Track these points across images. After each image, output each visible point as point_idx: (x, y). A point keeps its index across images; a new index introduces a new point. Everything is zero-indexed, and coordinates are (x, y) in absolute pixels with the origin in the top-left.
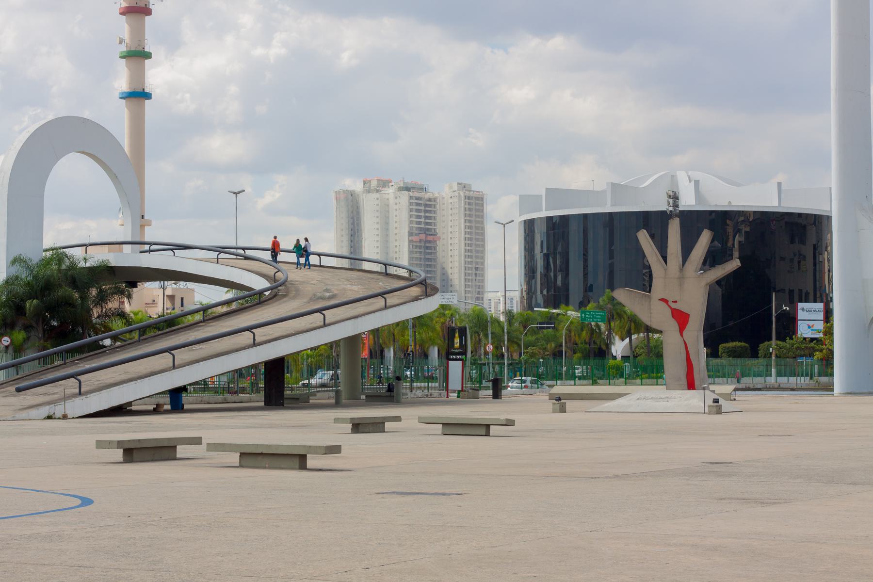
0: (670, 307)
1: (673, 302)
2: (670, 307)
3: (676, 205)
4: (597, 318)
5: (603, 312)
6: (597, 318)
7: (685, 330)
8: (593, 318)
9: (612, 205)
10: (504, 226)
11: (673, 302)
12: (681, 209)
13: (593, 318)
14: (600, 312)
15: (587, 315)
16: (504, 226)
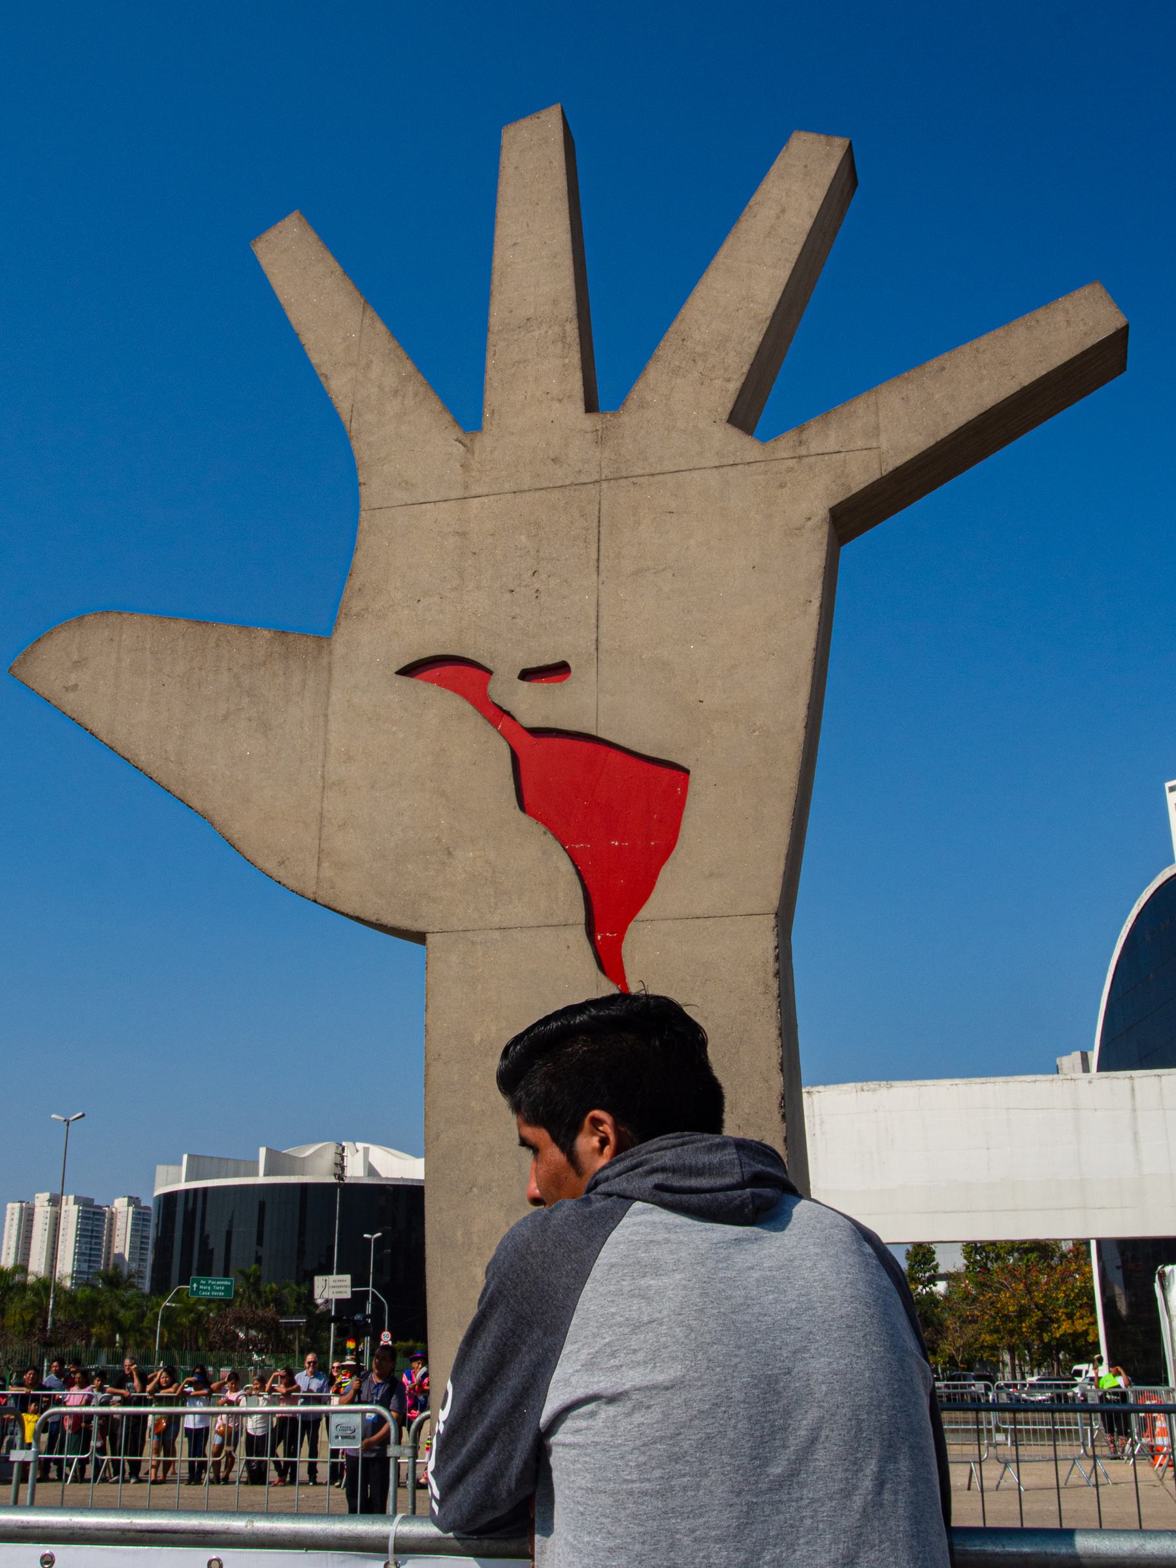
0: (498, 715)
1: (527, 675)
2: (498, 715)
3: (341, 1177)
4: (219, 1291)
5: (228, 1281)
6: (219, 1291)
7: (644, 913)
8: (212, 1289)
9: (265, 1175)
10: (68, 1125)
11: (527, 675)
12: (347, 1181)
13: (212, 1289)
14: (224, 1280)
15: (202, 1284)
16: (68, 1125)
